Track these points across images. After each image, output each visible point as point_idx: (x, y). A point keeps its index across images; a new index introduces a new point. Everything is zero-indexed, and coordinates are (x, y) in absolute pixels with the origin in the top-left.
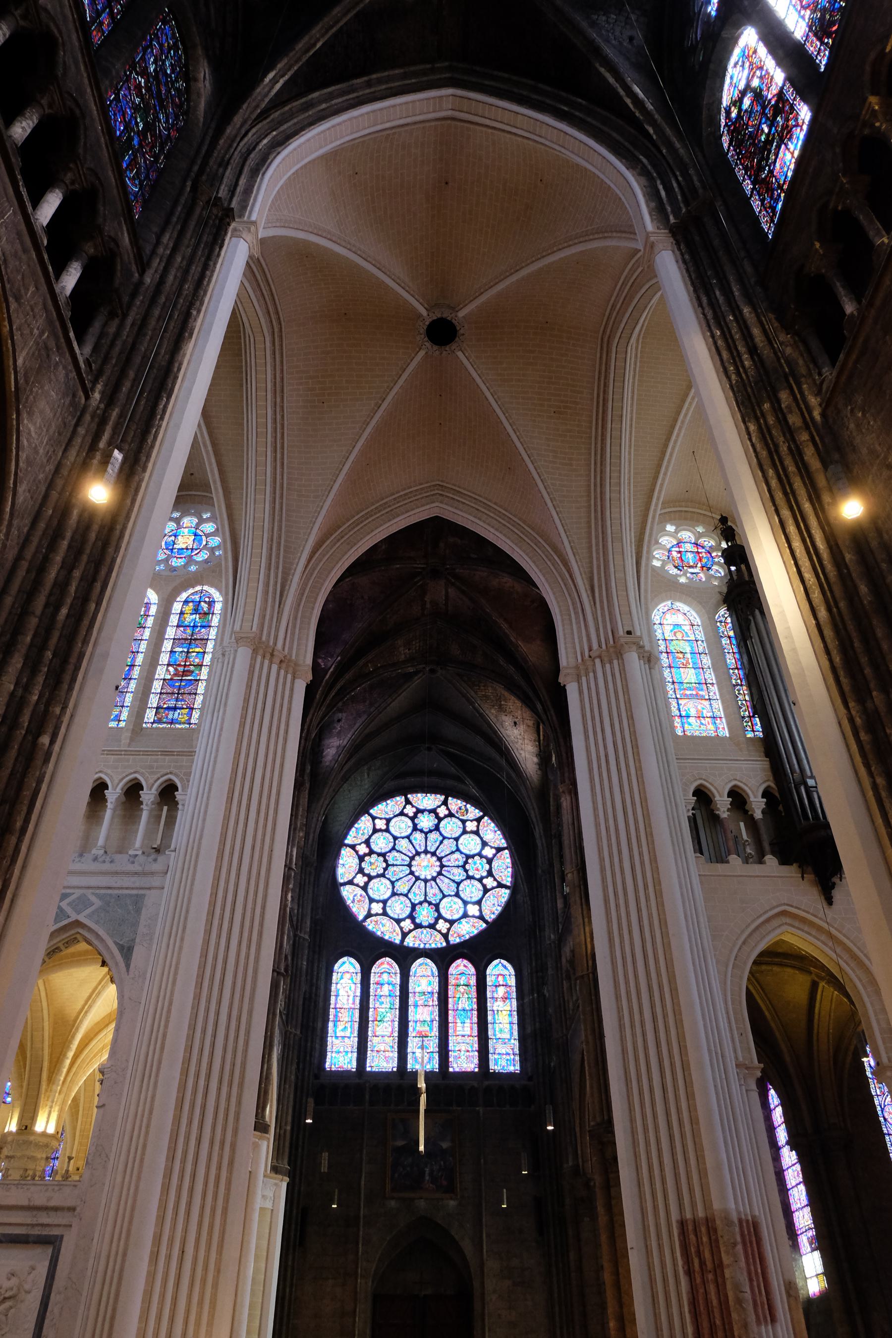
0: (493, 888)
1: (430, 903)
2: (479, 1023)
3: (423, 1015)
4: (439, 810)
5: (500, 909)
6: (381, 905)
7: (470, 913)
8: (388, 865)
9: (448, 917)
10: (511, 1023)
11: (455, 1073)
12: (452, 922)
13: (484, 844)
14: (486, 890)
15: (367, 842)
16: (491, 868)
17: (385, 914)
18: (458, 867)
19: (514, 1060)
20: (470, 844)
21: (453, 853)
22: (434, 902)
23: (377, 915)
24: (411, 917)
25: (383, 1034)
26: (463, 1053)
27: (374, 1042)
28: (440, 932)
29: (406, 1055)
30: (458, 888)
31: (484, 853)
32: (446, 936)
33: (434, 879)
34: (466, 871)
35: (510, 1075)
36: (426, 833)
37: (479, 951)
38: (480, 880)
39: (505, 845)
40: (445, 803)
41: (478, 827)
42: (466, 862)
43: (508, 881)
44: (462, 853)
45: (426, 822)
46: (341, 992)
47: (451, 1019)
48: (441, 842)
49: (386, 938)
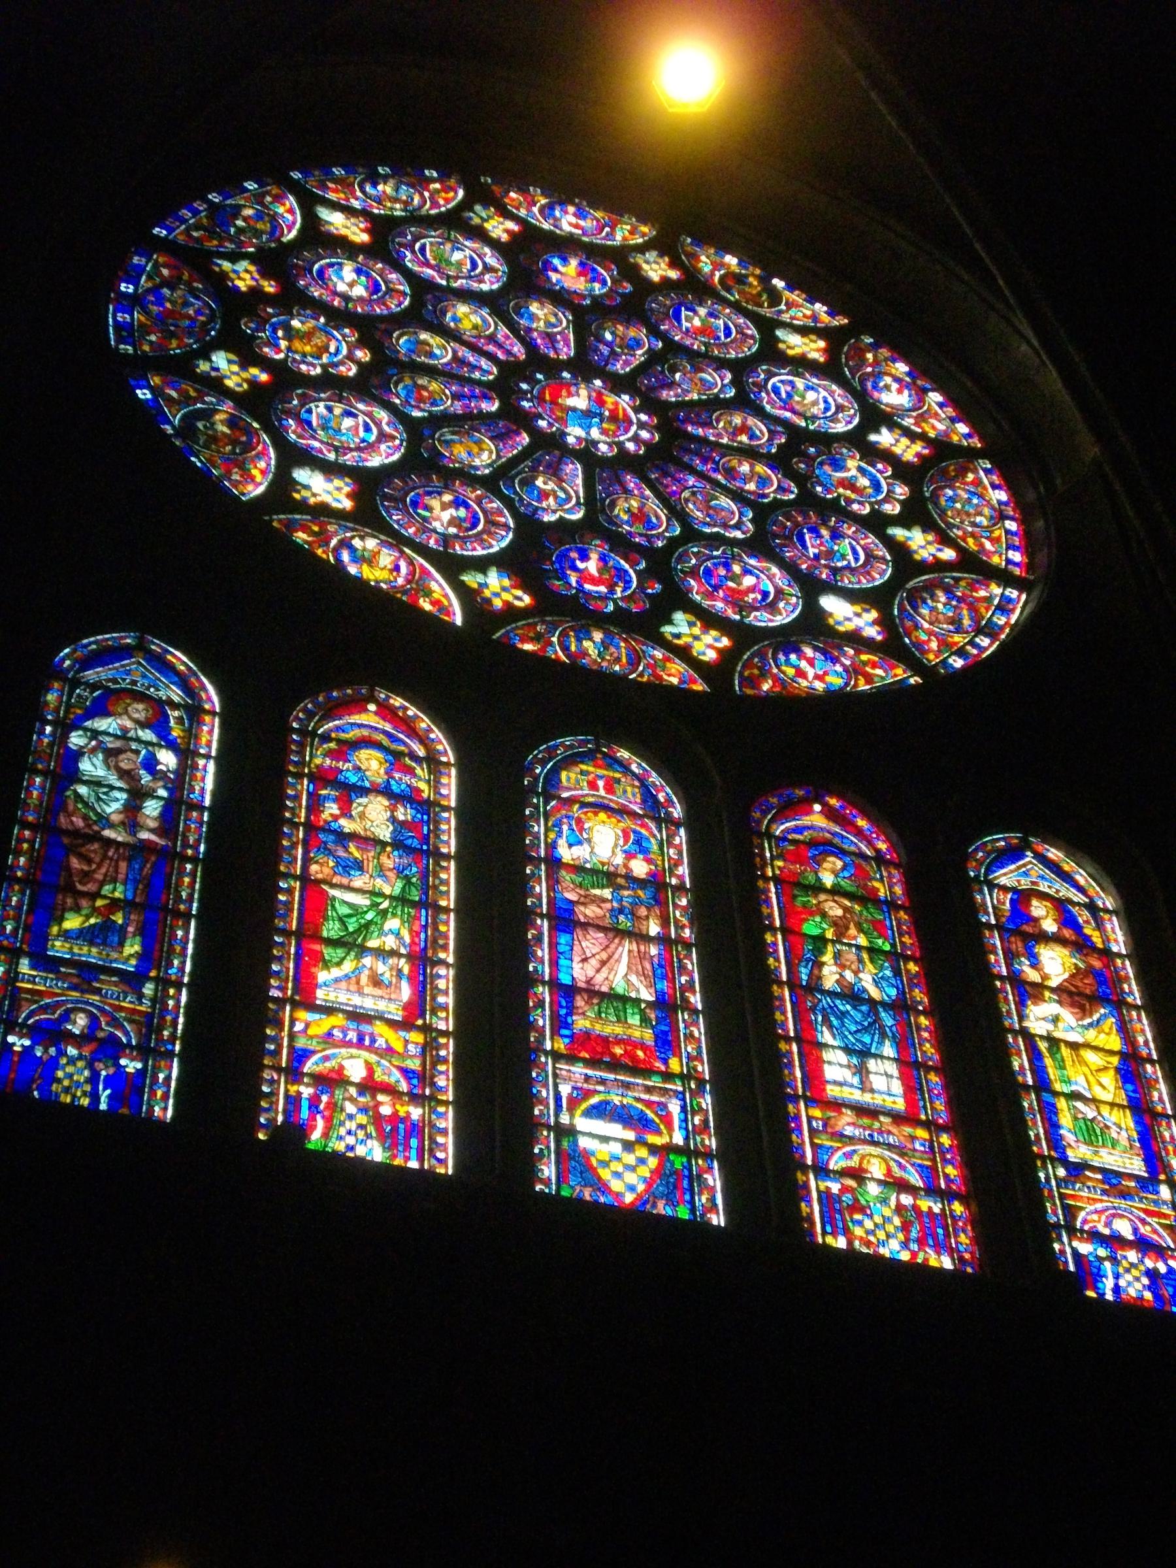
26: (873, 1189)
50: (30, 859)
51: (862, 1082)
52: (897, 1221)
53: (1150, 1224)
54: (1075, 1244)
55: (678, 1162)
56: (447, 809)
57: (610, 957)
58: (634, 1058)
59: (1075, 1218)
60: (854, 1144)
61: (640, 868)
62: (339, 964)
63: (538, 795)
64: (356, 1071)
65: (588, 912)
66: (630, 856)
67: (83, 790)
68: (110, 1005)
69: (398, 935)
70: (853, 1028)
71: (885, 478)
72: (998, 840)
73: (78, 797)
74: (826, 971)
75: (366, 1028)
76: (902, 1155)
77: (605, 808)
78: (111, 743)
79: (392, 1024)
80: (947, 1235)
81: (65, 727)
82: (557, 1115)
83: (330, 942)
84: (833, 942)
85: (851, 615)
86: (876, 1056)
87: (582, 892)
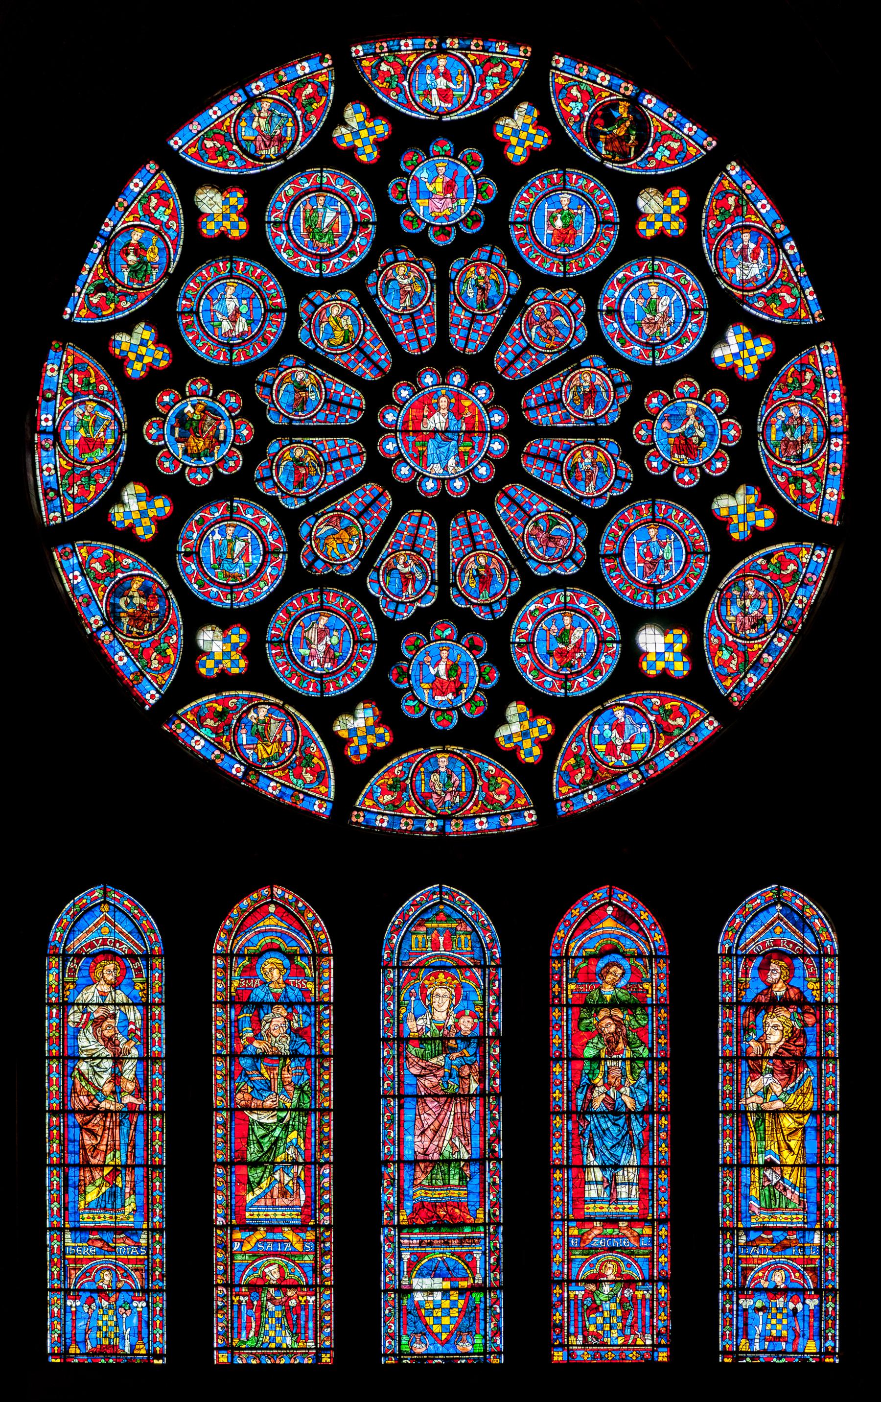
1: (465, 622)
3: (437, 1135)
4: (506, 127)
5: (782, 641)
6: (239, 636)
7: (651, 668)
8: (266, 432)
10: (818, 1166)
11: (572, 1367)
12: (564, 713)
13: (725, 310)
15: (161, 314)
16: (750, 436)
17: (259, 677)
19: (819, 1313)
21: (571, 359)
22: (483, 615)
23: (224, 681)
25: (274, 1213)
26: (607, 1288)
27: (243, 1255)
28: (509, 758)
29: (374, 1293)
30: (592, 543)
31: (722, 355)
32: (536, 779)
33: (481, 497)
34: (634, 454)
35: (801, 1372)
36: (442, 258)
37: (682, 848)
40: (533, 88)
41: (691, 214)
42: (634, 411)
43: (827, 502)
44: (614, 359)
46: (87, 1042)
47: (557, 1150)
48: (516, 305)
49: (272, 789)
50: (60, 1144)
51: (611, 1194)
52: (619, 1313)
53: (799, 1271)
54: (741, 1302)
55: (477, 1297)
57: (441, 1125)
58: (452, 1216)
59: (745, 1278)
60: (597, 1254)
61: (466, 1024)
62: (259, 1183)
63: (394, 968)
64: (273, 1274)
65: (427, 1083)
66: (460, 1015)
67: (84, 1066)
68: (122, 1260)
69: (297, 1147)
70: (609, 1144)
71: (720, 418)
72: (755, 899)
73: (81, 1074)
74: (595, 1094)
75: (278, 1236)
76: (628, 1256)
79: (295, 1228)
80: (652, 1317)
81: (65, 1005)
82: (400, 1280)
83: (255, 1164)
84: (606, 1059)
85: (661, 649)
86: (623, 1167)
87: (423, 1064)
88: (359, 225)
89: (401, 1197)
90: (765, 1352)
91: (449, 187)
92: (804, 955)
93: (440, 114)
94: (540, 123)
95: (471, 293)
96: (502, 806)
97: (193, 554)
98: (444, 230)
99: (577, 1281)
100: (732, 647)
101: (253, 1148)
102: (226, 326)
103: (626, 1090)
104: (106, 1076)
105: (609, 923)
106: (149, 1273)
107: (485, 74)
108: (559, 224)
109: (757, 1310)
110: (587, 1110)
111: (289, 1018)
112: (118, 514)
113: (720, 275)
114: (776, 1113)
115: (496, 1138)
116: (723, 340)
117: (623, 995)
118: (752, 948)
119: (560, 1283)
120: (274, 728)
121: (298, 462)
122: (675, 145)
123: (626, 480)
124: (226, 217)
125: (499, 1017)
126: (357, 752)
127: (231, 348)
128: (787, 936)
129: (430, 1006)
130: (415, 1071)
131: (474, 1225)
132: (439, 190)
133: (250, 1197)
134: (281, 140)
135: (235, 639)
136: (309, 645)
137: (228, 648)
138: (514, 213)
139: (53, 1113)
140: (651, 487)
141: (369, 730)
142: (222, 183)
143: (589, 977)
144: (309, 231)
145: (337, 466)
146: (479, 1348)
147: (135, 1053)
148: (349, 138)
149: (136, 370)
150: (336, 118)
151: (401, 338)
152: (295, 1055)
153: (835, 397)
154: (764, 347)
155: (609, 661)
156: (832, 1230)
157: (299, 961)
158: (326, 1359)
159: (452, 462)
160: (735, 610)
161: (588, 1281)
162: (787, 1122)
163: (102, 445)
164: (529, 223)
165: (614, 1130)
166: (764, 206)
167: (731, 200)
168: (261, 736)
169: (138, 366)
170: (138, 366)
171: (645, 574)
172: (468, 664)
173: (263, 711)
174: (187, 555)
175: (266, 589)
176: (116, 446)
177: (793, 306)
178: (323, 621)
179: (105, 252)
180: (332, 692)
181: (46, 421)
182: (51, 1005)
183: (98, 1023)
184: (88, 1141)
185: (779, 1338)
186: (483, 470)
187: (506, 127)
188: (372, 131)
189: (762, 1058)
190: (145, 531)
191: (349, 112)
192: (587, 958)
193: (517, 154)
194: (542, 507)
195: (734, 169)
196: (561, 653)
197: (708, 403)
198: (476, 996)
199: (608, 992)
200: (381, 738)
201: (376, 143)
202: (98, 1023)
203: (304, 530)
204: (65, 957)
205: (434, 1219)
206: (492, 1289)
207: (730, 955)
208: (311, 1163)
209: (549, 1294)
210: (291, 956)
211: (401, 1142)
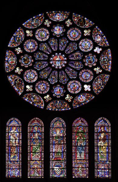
0: (100, 73)
2: (89, 153)
7: (86, 90)
9: (72, 92)
12: (74, 96)
14: (95, 75)
15: (22, 46)
17: (34, 91)
18: (78, 61)
20: (86, 45)
21: (75, 51)
23: (30, 92)
24: (50, 93)
26: (80, 168)
28: (67, 101)
32: (70, 104)
33: (63, 69)
34: (84, 63)
38: (92, 69)
39: (108, 45)
41: (91, 33)
42: (84, 58)
44: (81, 51)
45: (58, 31)
46: (12, 137)
47: (73, 151)
48: (68, 45)
49: (36, 105)
55: (63, 169)
56: (43, 132)
58: (59, 159)
61: (61, 135)
67: (11, 140)
75: (36, 162)
77: (58, 128)
78: (13, 134)
79: (39, 161)
81: (9, 133)
83: (33, 153)
88: (47, 35)
89: (53, 157)
90: (101, 177)
91: (59, 29)
92: (106, 126)
93: (58, 20)
94: (71, 22)
95: (62, 43)
96: (66, 107)
97: (26, 76)
98: (58, 35)
99: (76, 168)
100: (97, 87)
101: (33, 151)
102: (30, 47)
103: (82, 143)
104: (14, 141)
105: (80, 122)
106: (19, 166)
107: (64, 15)
108: (74, 34)
109: (100, 171)
110: (77, 146)
111: (38, 134)
112: (16, 71)
113: (95, 40)
114: (102, 146)
115: (65, 149)
116: (95, 49)
117: (82, 131)
118: (99, 125)
119: (74, 168)
120: (36, 98)
121: (39, 64)
122: (89, 24)
123: (82, 66)
124: (30, 34)
125: (65, 134)
126: (47, 100)
127: (30, 50)
128: (103, 123)
129: (56, 133)
130: (55, 141)
131: (62, 160)
132: (58, 31)
133: (33, 157)
134: (37, 24)
135: (31, 86)
136: (41, 87)
137: (30, 88)
138: (68, 33)
139: (7, 146)
140: (86, 68)
141: (49, 98)
142: (29, 30)
143: (78, 129)
144: (41, 35)
145: (44, 65)
146: (63, 176)
147: (18, 139)
148: (46, 24)
149: (18, 53)
150: (44, 21)
151: (53, 49)
152: (39, 139)
153: (110, 55)
154: (101, 49)
155: (80, 89)
156: (110, 161)
157: (39, 127)
158: (43, 177)
159: (59, 64)
160: (97, 82)
161: (77, 167)
162: (104, 147)
163: (14, 62)
164: (69, 34)
165: (81, 148)
166: (101, 31)
167: (96, 31)
168: (34, 99)
169: (18, 52)
170: (18, 52)
171: (85, 78)
172: (61, 89)
173: (35, 96)
174: (25, 76)
175: (35, 80)
176: (15, 62)
177: (105, 45)
178: (42, 84)
179: (14, 38)
180: (44, 93)
181: (6, 59)
182: (7, 133)
183: (13, 135)
184: (12, 150)
185: (103, 175)
186: (63, 65)
187: (67, 22)
188: (49, 23)
189: (100, 139)
190: (19, 73)
191: (46, 21)
192: (77, 127)
193: (68, 25)
194: (71, 70)
195: (97, 27)
196: (74, 88)
197: (93, 56)
198: (63, 131)
199: (80, 131)
200: (50, 99)
201: (49, 24)
202: (13, 135)
203: (40, 73)
204: (9, 127)
205: (57, 160)
206: (65, 168)
207: (96, 126)
208: (41, 153)
209: (72, 169)
210: (38, 126)
211: (53, 150)
